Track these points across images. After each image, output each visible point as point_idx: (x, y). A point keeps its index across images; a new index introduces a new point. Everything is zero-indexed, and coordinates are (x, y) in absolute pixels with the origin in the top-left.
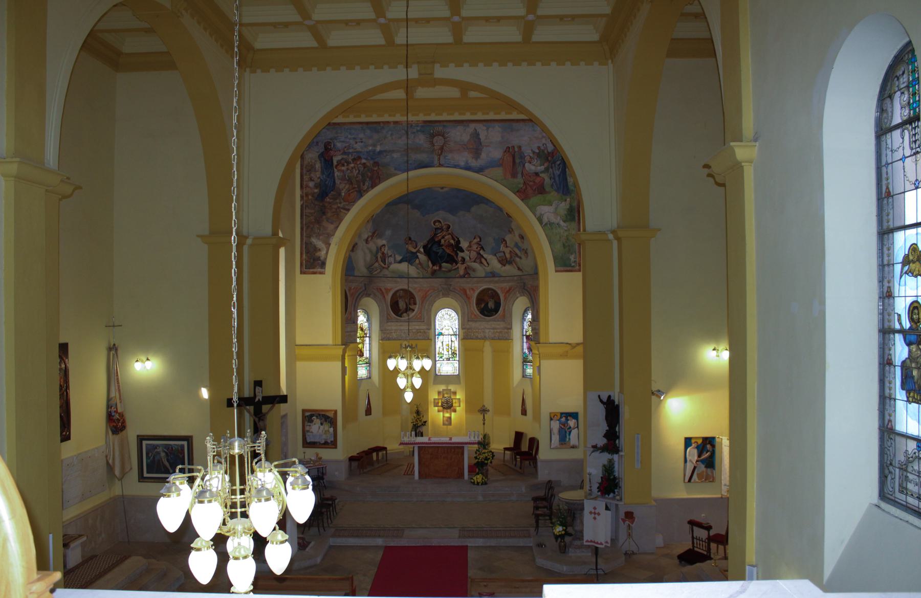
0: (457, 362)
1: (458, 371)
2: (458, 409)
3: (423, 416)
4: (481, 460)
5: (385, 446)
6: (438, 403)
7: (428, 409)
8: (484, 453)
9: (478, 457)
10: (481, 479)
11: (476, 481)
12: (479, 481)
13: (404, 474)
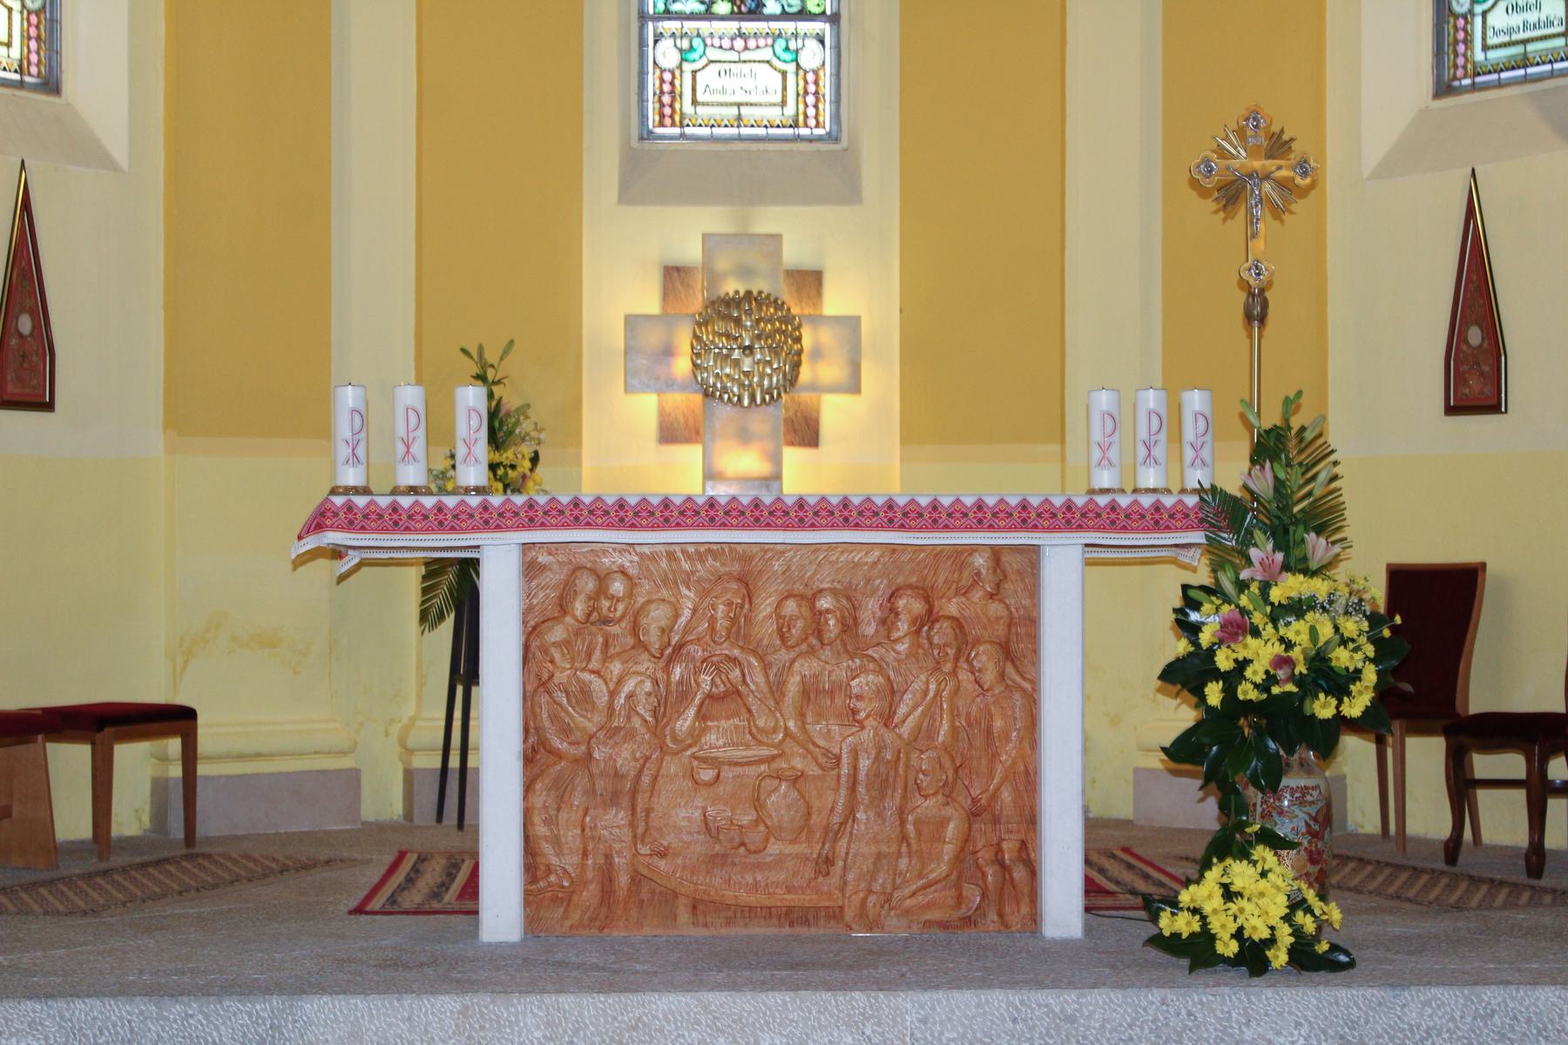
0: (827, 27)
1: (826, 109)
2: (834, 411)
3: (535, 460)
4: (1271, 679)
5: (182, 699)
6: (668, 352)
7: (573, 408)
8: (1298, 608)
9: (1224, 661)
10: (1278, 906)
11: (1222, 927)
12: (1258, 930)
13: (359, 910)
